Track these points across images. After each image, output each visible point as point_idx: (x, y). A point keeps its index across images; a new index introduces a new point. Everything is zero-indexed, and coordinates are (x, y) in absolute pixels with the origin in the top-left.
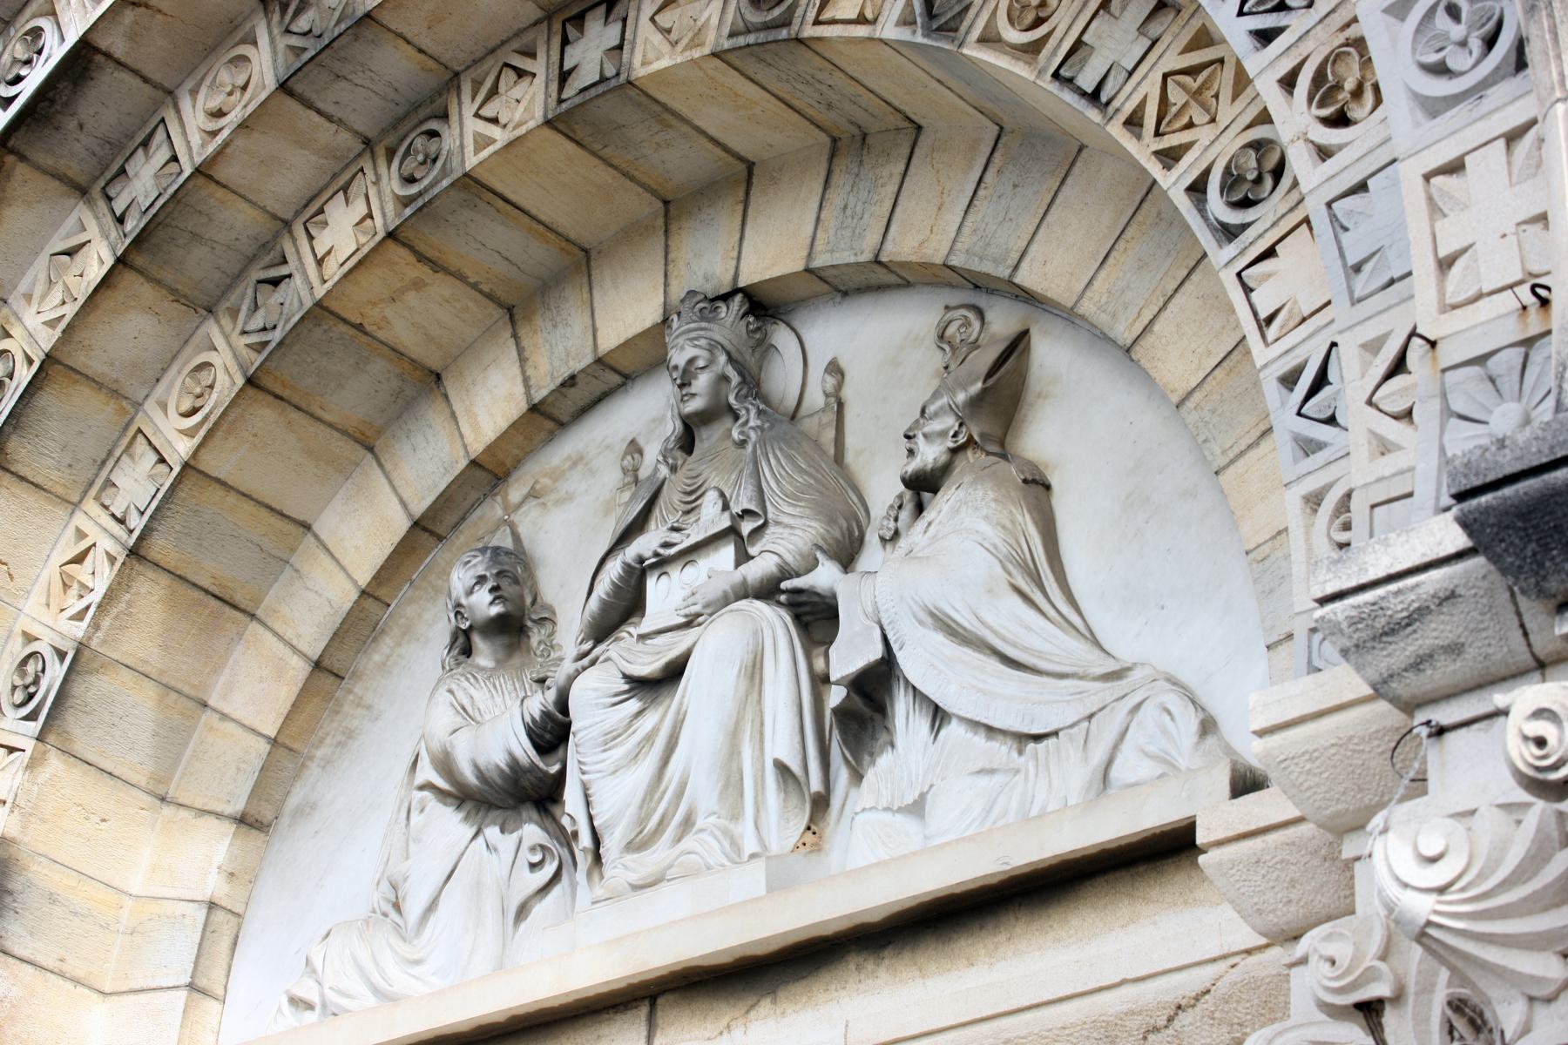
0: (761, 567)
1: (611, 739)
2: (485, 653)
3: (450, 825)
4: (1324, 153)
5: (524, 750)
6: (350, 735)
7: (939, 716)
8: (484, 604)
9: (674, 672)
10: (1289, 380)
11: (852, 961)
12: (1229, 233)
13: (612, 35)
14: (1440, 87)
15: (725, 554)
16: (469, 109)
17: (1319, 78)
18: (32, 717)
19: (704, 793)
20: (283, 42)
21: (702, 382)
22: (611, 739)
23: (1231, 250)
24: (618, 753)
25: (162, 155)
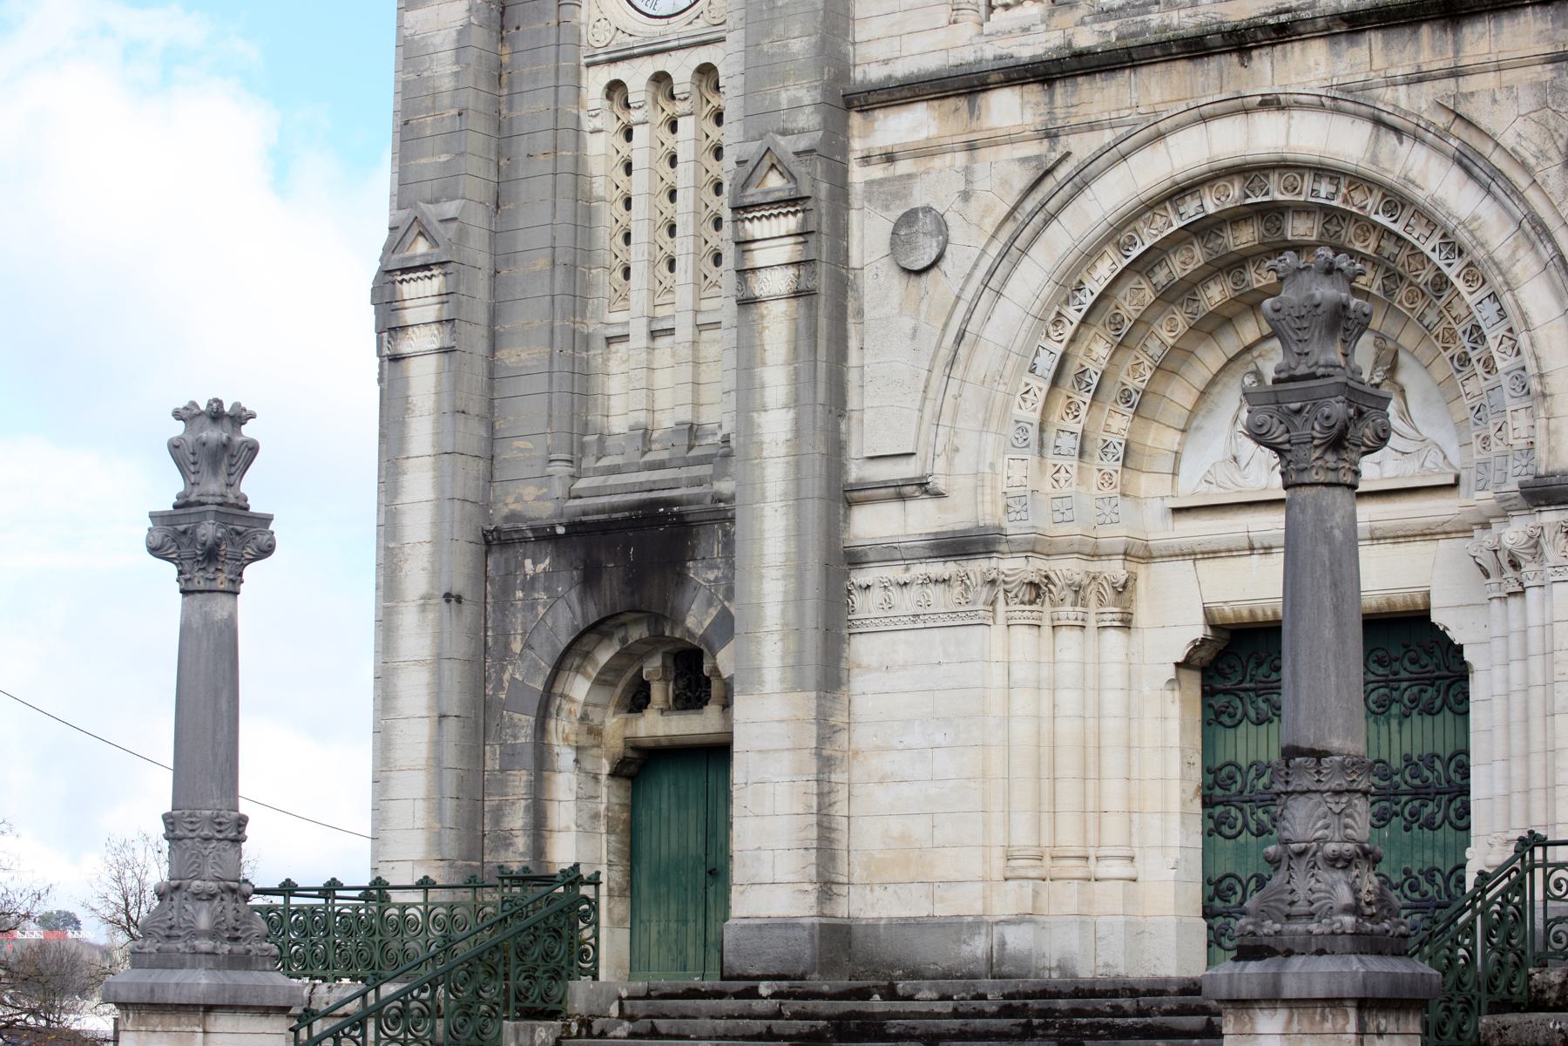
6: (1210, 411)
10: (1472, 408)
12: (1459, 371)
14: (1514, 394)
16: (1253, 270)
18: (1131, 407)
23: (1459, 376)
25: (1166, 271)
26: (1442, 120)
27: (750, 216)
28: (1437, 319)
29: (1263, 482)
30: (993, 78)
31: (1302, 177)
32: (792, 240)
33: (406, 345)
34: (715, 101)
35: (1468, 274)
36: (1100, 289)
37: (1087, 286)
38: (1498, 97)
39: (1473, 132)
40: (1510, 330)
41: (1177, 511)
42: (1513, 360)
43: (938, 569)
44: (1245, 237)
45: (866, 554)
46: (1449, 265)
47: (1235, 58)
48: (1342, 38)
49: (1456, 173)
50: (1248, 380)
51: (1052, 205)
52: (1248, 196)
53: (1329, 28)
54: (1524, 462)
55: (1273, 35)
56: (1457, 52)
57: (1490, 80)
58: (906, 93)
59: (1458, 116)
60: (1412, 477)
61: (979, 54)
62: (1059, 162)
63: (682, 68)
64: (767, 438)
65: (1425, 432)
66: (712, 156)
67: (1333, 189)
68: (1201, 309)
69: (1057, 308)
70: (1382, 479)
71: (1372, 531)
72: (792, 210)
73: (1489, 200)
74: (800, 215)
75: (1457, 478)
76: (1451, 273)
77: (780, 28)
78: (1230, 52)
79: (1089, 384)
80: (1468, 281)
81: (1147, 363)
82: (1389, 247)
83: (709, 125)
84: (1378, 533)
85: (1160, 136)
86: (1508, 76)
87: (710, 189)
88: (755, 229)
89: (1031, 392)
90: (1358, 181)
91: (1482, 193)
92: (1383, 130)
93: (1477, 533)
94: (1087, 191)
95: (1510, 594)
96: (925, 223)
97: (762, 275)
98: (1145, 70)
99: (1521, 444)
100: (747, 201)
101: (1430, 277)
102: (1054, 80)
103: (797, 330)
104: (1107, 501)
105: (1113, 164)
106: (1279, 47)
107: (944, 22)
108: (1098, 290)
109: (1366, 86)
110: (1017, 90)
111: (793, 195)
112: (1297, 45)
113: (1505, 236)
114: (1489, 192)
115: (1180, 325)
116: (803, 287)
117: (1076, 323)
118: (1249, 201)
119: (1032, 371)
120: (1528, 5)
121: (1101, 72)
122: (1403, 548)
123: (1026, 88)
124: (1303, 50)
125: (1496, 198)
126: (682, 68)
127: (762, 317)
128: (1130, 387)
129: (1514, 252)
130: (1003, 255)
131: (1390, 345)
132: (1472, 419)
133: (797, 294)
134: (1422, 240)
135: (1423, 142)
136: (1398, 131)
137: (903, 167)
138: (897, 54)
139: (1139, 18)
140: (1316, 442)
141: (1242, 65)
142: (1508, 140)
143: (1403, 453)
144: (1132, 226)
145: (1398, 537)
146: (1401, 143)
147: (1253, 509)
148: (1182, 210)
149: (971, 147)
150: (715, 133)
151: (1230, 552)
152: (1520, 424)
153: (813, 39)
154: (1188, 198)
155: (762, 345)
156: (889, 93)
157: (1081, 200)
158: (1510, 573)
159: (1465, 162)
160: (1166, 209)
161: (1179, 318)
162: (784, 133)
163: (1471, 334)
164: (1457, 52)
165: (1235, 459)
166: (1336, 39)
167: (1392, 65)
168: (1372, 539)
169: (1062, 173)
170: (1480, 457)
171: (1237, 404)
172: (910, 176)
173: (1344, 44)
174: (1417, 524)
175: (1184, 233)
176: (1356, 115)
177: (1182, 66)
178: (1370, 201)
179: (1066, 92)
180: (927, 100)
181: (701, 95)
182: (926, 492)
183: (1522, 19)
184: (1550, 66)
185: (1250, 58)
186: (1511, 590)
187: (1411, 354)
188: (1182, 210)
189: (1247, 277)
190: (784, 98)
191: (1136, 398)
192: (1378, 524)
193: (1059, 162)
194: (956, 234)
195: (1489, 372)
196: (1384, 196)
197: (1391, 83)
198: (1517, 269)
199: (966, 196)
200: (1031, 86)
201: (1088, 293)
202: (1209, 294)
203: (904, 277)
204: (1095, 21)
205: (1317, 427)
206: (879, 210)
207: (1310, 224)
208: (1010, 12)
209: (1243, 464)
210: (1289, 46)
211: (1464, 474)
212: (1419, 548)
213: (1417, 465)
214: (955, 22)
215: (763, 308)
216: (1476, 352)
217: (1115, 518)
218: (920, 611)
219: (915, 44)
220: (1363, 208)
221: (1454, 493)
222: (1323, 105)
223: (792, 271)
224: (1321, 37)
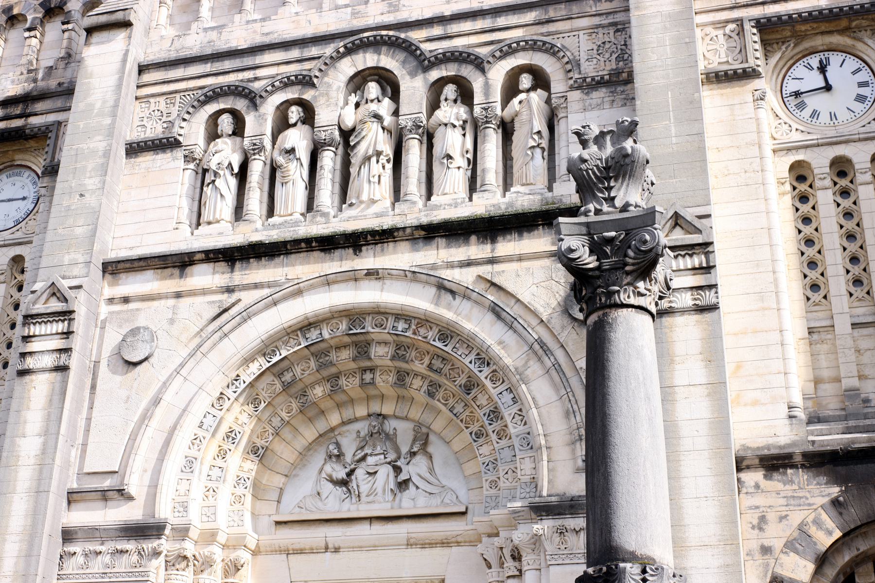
0: (388, 460)
1: (363, 480)
2: (334, 459)
3: (330, 486)
4: (498, 443)
5: (345, 477)
6: (305, 465)
7: (417, 488)
8: (336, 452)
9: (376, 473)
10: (484, 463)
11: (404, 519)
12: (475, 441)
13: (372, 376)
14: (521, 448)
15: (382, 457)
16: (344, 379)
17: (497, 433)
18: (258, 456)
19: (379, 490)
20: (317, 363)
21: (377, 428)
22: (363, 480)
23: (476, 443)
24: (365, 482)
25: (291, 374)
27: (34, 321)
28: (463, 410)
29: (337, 508)
30: (198, 257)
31: (387, 319)
32: (59, 336)
34: (20, 278)
35: (493, 376)
36: (251, 380)
37: (242, 378)
38: (520, 273)
39: (502, 293)
40: (520, 410)
41: (278, 523)
42: (521, 428)
45: (76, 533)
46: (480, 371)
47: (351, 251)
48: (420, 241)
49: (490, 317)
50: (331, 447)
51: (226, 329)
52: (351, 329)
53: (413, 234)
54: (528, 490)
55: (377, 238)
56: (493, 251)
57: (515, 266)
58: (142, 263)
59: (493, 284)
60: (437, 506)
61: (190, 246)
62: (233, 305)
64: (22, 454)
65: (444, 482)
66: (12, 308)
67: (407, 326)
68: (308, 400)
69: (221, 390)
70: (415, 507)
71: (408, 540)
72: (62, 318)
73: (511, 332)
74: (66, 322)
75: (467, 509)
76: (482, 376)
77: (70, 221)
78: (348, 247)
79: (233, 439)
80: (492, 381)
81: (271, 431)
82: (437, 364)
83: (14, 291)
84: (412, 541)
86: (525, 264)
87: (9, 325)
89: (198, 439)
90: (424, 321)
91: (507, 328)
92: (443, 292)
93: (485, 539)
94: (249, 322)
95: (508, 577)
96: (146, 336)
97: (36, 357)
98: (293, 256)
99: (526, 479)
100: (34, 312)
101: (463, 382)
102: (235, 260)
103: (53, 390)
104: (236, 512)
105: (267, 307)
106: (380, 245)
107: (171, 228)
108: (248, 380)
110: (212, 265)
111: (65, 309)
112: (391, 244)
113: (521, 353)
114: (511, 327)
115: (294, 409)
116: (61, 363)
117: (232, 399)
118: (351, 332)
119: (200, 427)
120: (539, 225)
121: (265, 256)
122: (427, 551)
123: (217, 264)
124: (394, 247)
125: (515, 331)
127: (32, 381)
128: (258, 445)
129: (526, 362)
130: (191, 355)
131: (424, 430)
132: (483, 470)
134: (463, 356)
135: (469, 298)
136: (453, 293)
137: (132, 306)
138: (139, 245)
139: (292, 229)
140: (628, 268)
141: (355, 254)
142: (525, 297)
143: (431, 494)
144: (274, 344)
145: (425, 544)
146: (454, 299)
147: (329, 524)
148: (308, 336)
150: (16, 295)
151: (312, 551)
153: (90, 227)
154: (312, 329)
155: (29, 398)
156: (131, 264)
157: (245, 326)
158: (510, 563)
159: (496, 311)
160: (297, 335)
161: (294, 405)
162: (63, 278)
163: (489, 415)
164: (493, 251)
165: (319, 494)
166: (416, 241)
167: (451, 256)
168: (408, 545)
170: (488, 492)
171: (323, 462)
172: (138, 310)
173: (421, 244)
174: (439, 536)
175: (306, 351)
176: (427, 283)
177: (316, 254)
178: (430, 334)
179: (242, 267)
180: (154, 269)
181: (12, 274)
182: (122, 495)
183: (536, 232)
184: (553, 258)
185: (361, 251)
186: (511, 574)
187: (439, 435)
188: (308, 336)
189: (340, 383)
190: (66, 259)
191: (261, 451)
192: (413, 535)
193: (233, 305)
195: (500, 439)
196: (440, 331)
197: (450, 265)
198: (528, 372)
199: (172, 321)
200: (220, 263)
201: (242, 382)
202: (315, 392)
203: (126, 367)
204: (264, 230)
205: (631, 253)
206: (115, 328)
207: (386, 350)
208: (211, 226)
209: (324, 497)
210: (386, 245)
211: (470, 506)
212: (438, 551)
213: (439, 501)
214: (177, 229)
215: (33, 377)
216: (492, 426)
217: (240, 523)
218: (108, 571)
220: (426, 338)
221: (463, 518)
222: (406, 276)
223: (56, 355)
224: (407, 240)
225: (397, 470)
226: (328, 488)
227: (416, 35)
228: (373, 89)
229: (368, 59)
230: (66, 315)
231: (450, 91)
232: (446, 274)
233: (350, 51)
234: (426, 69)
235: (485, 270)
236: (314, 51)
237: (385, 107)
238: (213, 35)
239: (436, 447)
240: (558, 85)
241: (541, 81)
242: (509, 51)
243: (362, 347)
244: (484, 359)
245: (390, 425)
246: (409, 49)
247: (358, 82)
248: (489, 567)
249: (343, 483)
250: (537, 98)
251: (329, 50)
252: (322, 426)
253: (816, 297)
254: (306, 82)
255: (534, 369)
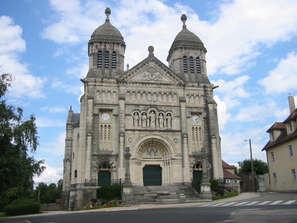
26: (166, 137)
33: (87, 141)
43: (132, 161)
44: (151, 142)
63: (107, 125)
85: (148, 136)
88: (121, 137)
90: (160, 140)
109: (161, 135)
126: (107, 125)
133: (124, 142)
149: (134, 134)
152: (170, 155)
169: (141, 137)
194: (133, 139)
219: (129, 127)
225: (155, 153)
226: (148, 155)
227: (158, 107)
228: (153, 112)
229: (152, 109)
230: (124, 136)
231: (161, 114)
232: (163, 136)
233: (150, 107)
234: (159, 112)
235: (166, 136)
236: (146, 107)
237: (154, 115)
238: (133, 101)
239: (158, 151)
240: (172, 116)
241: (170, 115)
242: (167, 111)
243: (153, 141)
244: (166, 144)
245: (154, 149)
246: (157, 108)
247: (151, 111)
248: (165, 163)
249: (149, 154)
250: (170, 117)
251: (148, 107)
252: (147, 148)
253: (193, 140)
254: (146, 111)
255: (171, 146)
